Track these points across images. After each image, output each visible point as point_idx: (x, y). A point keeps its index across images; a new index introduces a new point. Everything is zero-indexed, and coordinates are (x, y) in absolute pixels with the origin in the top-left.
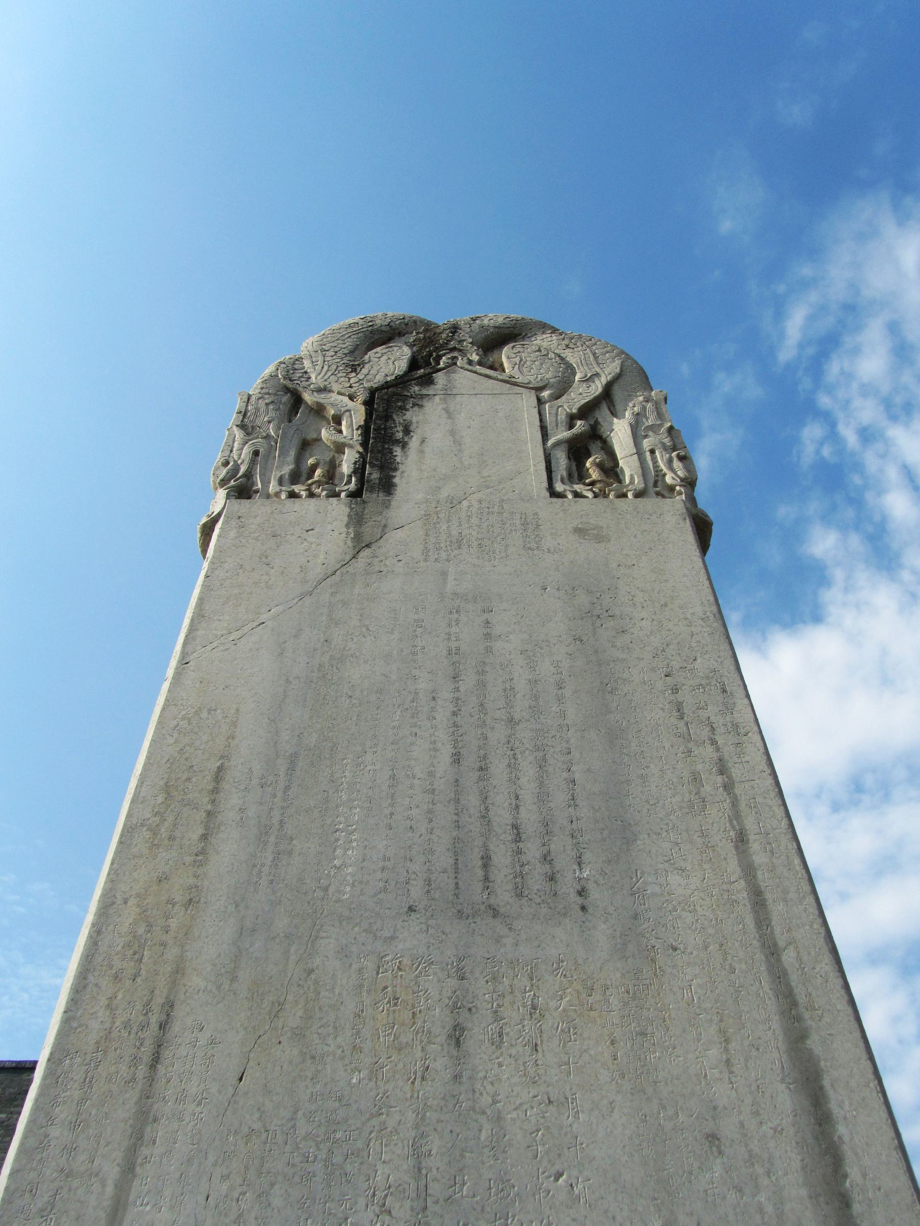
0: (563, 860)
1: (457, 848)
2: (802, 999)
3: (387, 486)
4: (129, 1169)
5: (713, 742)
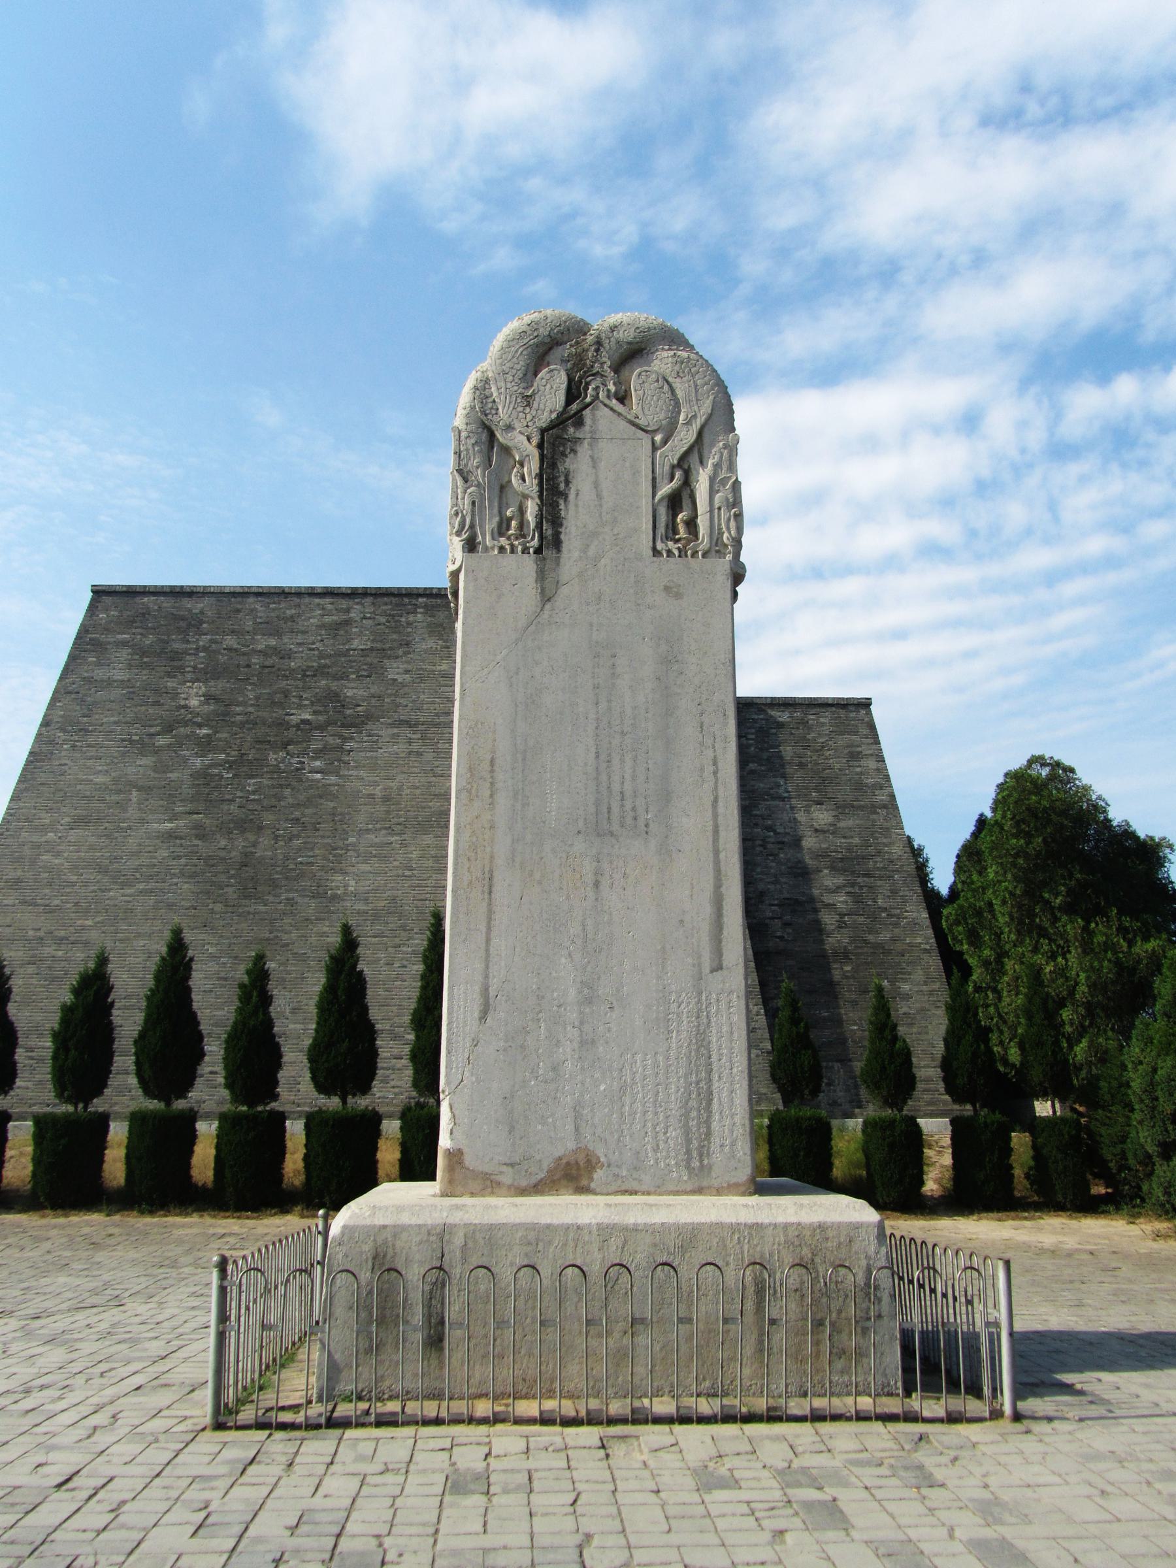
0: (641, 810)
1: (597, 803)
2: (723, 873)
3: (557, 543)
4: (489, 929)
5: (714, 747)
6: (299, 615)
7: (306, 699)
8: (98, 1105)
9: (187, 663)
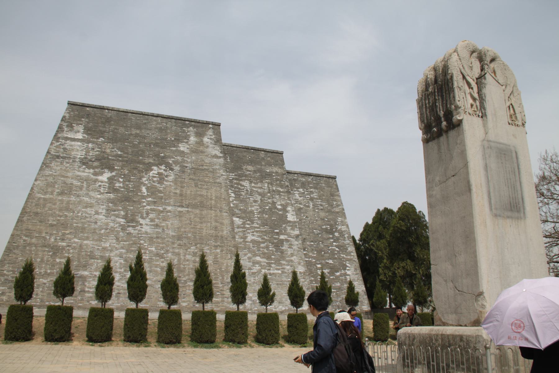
3: (486, 115)
6: (148, 123)
7: (151, 154)
8: (29, 303)
9: (105, 136)
